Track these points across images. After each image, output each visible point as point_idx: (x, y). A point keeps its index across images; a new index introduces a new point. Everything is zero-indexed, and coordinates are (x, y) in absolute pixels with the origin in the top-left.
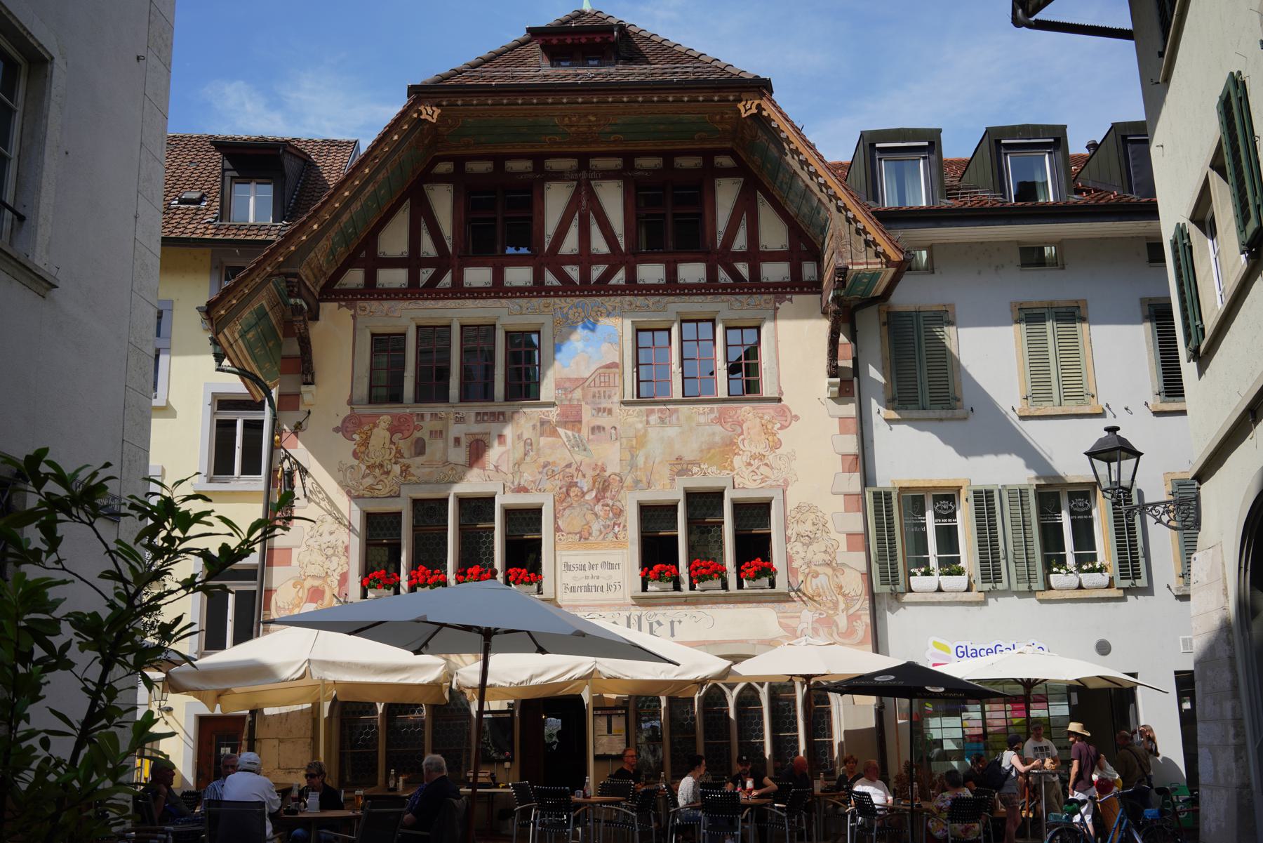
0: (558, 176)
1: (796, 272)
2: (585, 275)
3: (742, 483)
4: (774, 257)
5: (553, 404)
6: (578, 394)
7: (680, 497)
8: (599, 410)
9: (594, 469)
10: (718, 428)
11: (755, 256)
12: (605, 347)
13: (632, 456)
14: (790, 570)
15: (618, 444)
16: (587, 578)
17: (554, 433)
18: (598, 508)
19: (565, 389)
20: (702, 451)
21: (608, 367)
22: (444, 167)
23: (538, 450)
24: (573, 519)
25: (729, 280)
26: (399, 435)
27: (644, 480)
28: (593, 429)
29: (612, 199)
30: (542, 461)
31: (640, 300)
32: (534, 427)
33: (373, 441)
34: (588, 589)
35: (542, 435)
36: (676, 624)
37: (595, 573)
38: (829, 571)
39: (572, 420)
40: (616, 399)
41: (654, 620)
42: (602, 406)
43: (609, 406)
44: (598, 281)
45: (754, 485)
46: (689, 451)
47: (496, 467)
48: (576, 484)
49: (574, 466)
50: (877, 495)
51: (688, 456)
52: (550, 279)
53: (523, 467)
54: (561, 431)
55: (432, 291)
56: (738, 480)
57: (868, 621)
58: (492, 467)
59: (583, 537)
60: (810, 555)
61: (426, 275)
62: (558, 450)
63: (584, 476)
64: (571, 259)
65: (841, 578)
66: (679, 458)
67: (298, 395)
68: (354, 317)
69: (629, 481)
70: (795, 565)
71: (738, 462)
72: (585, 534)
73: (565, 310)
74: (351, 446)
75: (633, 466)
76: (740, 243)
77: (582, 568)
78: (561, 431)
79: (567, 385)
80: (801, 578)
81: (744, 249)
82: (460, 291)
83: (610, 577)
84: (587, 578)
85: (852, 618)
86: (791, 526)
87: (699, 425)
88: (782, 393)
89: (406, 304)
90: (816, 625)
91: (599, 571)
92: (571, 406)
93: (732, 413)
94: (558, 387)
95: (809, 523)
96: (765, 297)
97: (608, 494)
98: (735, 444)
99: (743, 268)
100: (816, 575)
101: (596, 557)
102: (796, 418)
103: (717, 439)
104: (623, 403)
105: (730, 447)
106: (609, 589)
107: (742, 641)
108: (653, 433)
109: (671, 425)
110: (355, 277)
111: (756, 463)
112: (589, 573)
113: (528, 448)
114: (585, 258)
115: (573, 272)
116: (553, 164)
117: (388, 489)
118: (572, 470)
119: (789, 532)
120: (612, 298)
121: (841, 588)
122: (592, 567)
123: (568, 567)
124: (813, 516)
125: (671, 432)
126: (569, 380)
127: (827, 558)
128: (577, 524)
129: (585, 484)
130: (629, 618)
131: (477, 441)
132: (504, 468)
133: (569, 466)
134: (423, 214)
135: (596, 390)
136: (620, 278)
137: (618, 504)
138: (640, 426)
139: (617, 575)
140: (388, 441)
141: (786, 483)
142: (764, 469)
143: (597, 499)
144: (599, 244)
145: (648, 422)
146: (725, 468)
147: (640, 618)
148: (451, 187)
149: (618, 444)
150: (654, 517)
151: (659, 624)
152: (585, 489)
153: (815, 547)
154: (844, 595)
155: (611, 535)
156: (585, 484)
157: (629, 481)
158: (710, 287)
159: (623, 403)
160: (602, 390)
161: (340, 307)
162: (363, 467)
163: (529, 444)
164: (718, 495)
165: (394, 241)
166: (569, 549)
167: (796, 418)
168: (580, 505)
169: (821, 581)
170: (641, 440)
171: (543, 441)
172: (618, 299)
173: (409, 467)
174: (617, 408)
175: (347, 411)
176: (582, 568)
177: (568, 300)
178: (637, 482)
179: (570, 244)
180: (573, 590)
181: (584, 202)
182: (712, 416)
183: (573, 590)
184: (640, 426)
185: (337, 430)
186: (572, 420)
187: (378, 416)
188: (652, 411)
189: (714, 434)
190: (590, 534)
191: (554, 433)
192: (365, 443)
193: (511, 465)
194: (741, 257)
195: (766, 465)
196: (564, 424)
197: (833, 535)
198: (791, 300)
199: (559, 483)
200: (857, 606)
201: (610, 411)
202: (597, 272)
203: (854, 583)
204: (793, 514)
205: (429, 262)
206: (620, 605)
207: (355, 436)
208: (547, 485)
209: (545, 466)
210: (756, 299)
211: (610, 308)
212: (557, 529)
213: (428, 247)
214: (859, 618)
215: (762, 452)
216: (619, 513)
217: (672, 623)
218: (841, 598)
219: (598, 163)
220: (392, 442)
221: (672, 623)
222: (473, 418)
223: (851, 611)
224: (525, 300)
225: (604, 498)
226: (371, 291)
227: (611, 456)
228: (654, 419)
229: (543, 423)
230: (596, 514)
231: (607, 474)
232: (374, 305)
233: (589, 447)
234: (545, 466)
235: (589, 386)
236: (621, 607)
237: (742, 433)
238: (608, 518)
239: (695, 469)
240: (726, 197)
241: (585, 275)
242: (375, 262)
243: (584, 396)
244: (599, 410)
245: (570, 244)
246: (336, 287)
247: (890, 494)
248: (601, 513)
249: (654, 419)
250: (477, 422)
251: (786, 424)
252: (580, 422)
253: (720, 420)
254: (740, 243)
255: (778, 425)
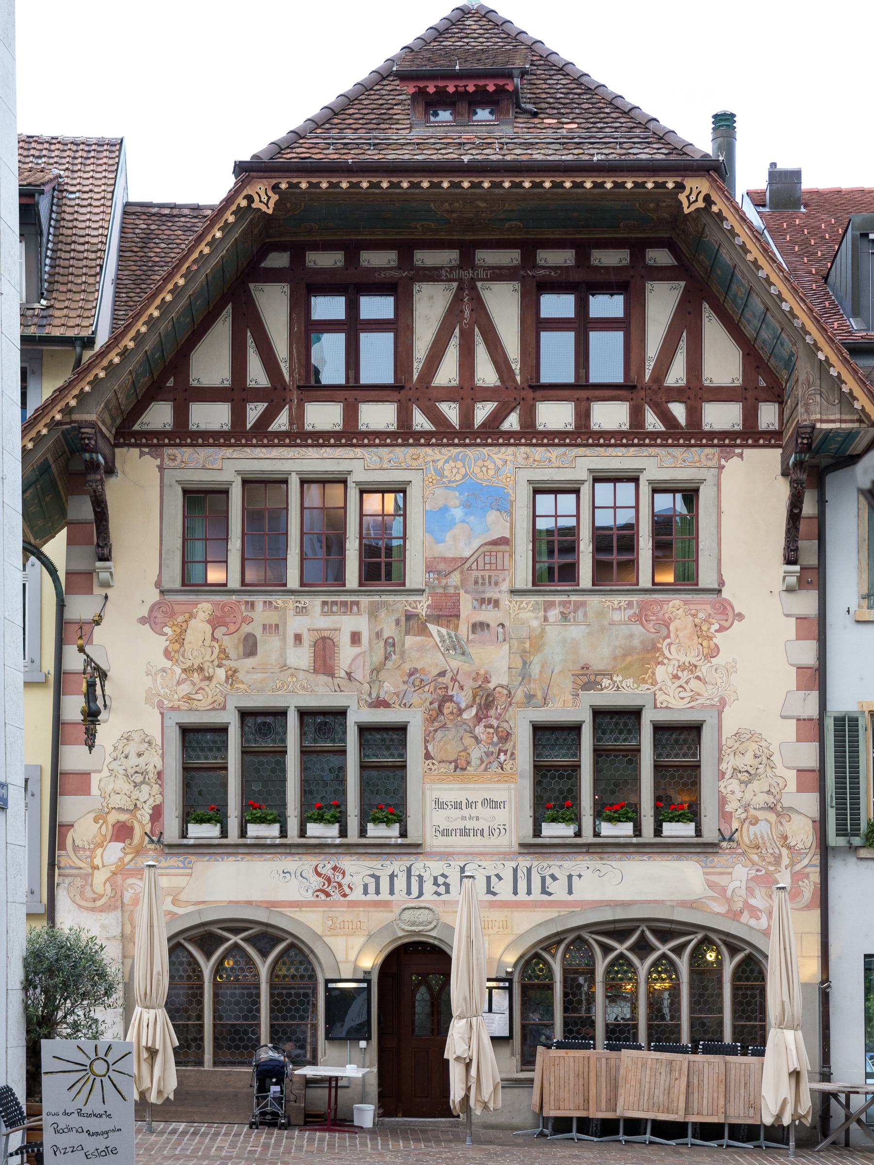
0: (432, 275)
1: (750, 416)
2: (467, 416)
3: (666, 698)
4: (722, 394)
5: (421, 592)
6: (455, 579)
7: (586, 717)
8: (483, 601)
9: (475, 680)
10: (637, 629)
11: (696, 393)
12: (492, 516)
13: (525, 663)
14: (725, 816)
15: (506, 647)
16: (464, 818)
17: (423, 631)
18: (479, 730)
19: (439, 572)
20: (615, 658)
21: (495, 543)
22: (279, 260)
23: (403, 653)
24: (447, 744)
25: (661, 427)
26: (223, 629)
27: (539, 694)
28: (474, 626)
29: (503, 305)
30: (407, 667)
31: (539, 453)
32: (398, 622)
33: (189, 637)
34: (465, 832)
35: (407, 633)
36: (575, 879)
37: (473, 812)
38: (772, 817)
39: (446, 613)
40: (505, 586)
41: (547, 873)
42: (487, 595)
43: (495, 596)
44: (484, 425)
45: (682, 704)
46: (599, 656)
47: (349, 674)
48: (450, 699)
49: (449, 675)
50: (840, 721)
51: (597, 664)
52: (420, 421)
53: (383, 675)
54: (432, 628)
55: (261, 435)
56: (660, 697)
57: (818, 880)
58: (343, 674)
59: (460, 766)
60: (748, 796)
61: (254, 412)
62: (428, 653)
63: (462, 688)
64: (449, 394)
65: (787, 826)
66: (585, 667)
67: (90, 574)
68: (161, 468)
69: (519, 695)
70: (729, 808)
71: (661, 673)
72: (462, 763)
73: (440, 464)
74: (161, 643)
75: (525, 675)
76: (677, 375)
77: (457, 806)
78: (432, 628)
79: (442, 566)
80: (735, 825)
81: (683, 383)
82: (300, 437)
83: (494, 818)
84: (464, 818)
85: (797, 877)
86: (726, 758)
87: (612, 623)
88: (722, 583)
89: (228, 452)
90: (751, 884)
91: (480, 811)
92: (446, 595)
93: (656, 608)
94: (429, 569)
95: (750, 755)
96: (708, 450)
97: (492, 712)
98: (659, 650)
99: (678, 410)
100: (755, 821)
101: (477, 792)
102: (740, 616)
103: (636, 642)
104: (513, 592)
105: (651, 653)
106: (491, 833)
107: (656, 902)
108: (553, 633)
109: (576, 623)
110: (159, 416)
111: (684, 676)
112: (466, 812)
113: (389, 649)
114: (467, 392)
115: (451, 412)
116: (425, 258)
117: (210, 700)
118: (446, 680)
119: (723, 766)
120: (503, 449)
121: (786, 838)
122: (469, 805)
123: (440, 804)
124: (754, 746)
125: (576, 632)
126: (444, 559)
127: (770, 799)
128: (452, 750)
129: (463, 698)
130: (515, 871)
131: (324, 639)
132: (358, 675)
133: (442, 674)
134: (249, 323)
135: (479, 574)
136: (512, 422)
137: (505, 725)
138: (535, 624)
139: (502, 816)
140: (209, 637)
141: (723, 702)
142: (694, 684)
143: (478, 719)
144: (486, 374)
145: (546, 619)
146: (644, 681)
147: (529, 870)
148: (287, 288)
149: (506, 647)
150: (551, 736)
151: (554, 878)
152: (463, 706)
153: (755, 786)
154: (789, 848)
155: (495, 764)
156: (463, 698)
157: (519, 695)
158: (634, 436)
159: (513, 592)
160: (487, 574)
161: (142, 454)
162: (178, 671)
163: (390, 644)
164: (636, 713)
165: (211, 365)
166: (441, 781)
167: (740, 616)
168: (456, 726)
169: (762, 830)
170: (537, 642)
171: (410, 640)
172: (511, 450)
173: (235, 671)
174: (505, 600)
175: (154, 596)
176: (457, 806)
177: (444, 450)
178: (530, 697)
179: (447, 373)
180: (446, 833)
181: (467, 313)
182: (630, 612)
183: (446, 833)
184: (535, 624)
185: (143, 621)
186: (446, 613)
187: (196, 604)
188: (551, 604)
189: (631, 636)
190: (468, 763)
191: (423, 631)
192: (180, 639)
193: (368, 672)
194: (678, 394)
195: (698, 678)
196: (437, 619)
197: (780, 770)
198: (741, 455)
199: (430, 698)
200: (805, 862)
201: (496, 603)
202: (482, 412)
203: (802, 832)
204: (730, 743)
205: (258, 395)
206: (504, 854)
207: (167, 630)
208: (415, 699)
209: (411, 674)
210: (695, 453)
211: (499, 463)
212: (428, 756)
213: (257, 375)
214: (807, 876)
215: (694, 661)
216: (506, 737)
217: (570, 877)
218: (784, 851)
219: (487, 257)
220: (214, 639)
221: (570, 877)
222: (318, 609)
223: (798, 867)
224: (386, 450)
225: (486, 717)
226: (182, 434)
227: (496, 662)
228: (554, 614)
229: (409, 617)
230: (476, 738)
231: (491, 686)
232: (186, 454)
233: (470, 650)
234: (411, 674)
235: (470, 569)
236: (505, 856)
237: (668, 636)
238: (492, 743)
239: (606, 682)
240: (661, 303)
241: (467, 416)
242: (186, 396)
243: (463, 581)
244: (483, 601)
245: (447, 373)
246: (136, 427)
247: (857, 720)
248: (483, 737)
249: (554, 614)
250: (324, 613)
251: (726, 624)
252: (458, 616)
253: (640, 618)
254: (677, 375)
255: (716, 626)
